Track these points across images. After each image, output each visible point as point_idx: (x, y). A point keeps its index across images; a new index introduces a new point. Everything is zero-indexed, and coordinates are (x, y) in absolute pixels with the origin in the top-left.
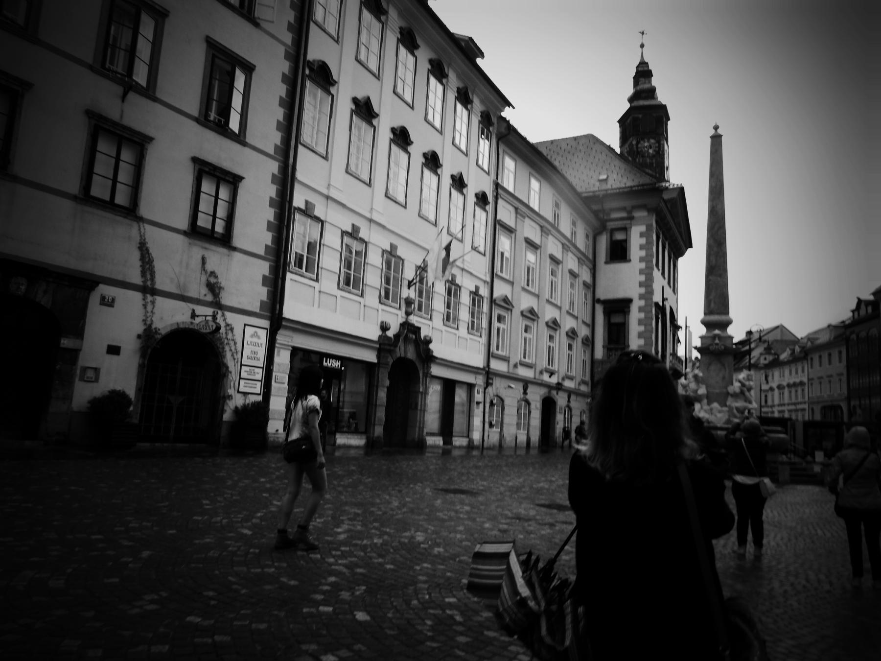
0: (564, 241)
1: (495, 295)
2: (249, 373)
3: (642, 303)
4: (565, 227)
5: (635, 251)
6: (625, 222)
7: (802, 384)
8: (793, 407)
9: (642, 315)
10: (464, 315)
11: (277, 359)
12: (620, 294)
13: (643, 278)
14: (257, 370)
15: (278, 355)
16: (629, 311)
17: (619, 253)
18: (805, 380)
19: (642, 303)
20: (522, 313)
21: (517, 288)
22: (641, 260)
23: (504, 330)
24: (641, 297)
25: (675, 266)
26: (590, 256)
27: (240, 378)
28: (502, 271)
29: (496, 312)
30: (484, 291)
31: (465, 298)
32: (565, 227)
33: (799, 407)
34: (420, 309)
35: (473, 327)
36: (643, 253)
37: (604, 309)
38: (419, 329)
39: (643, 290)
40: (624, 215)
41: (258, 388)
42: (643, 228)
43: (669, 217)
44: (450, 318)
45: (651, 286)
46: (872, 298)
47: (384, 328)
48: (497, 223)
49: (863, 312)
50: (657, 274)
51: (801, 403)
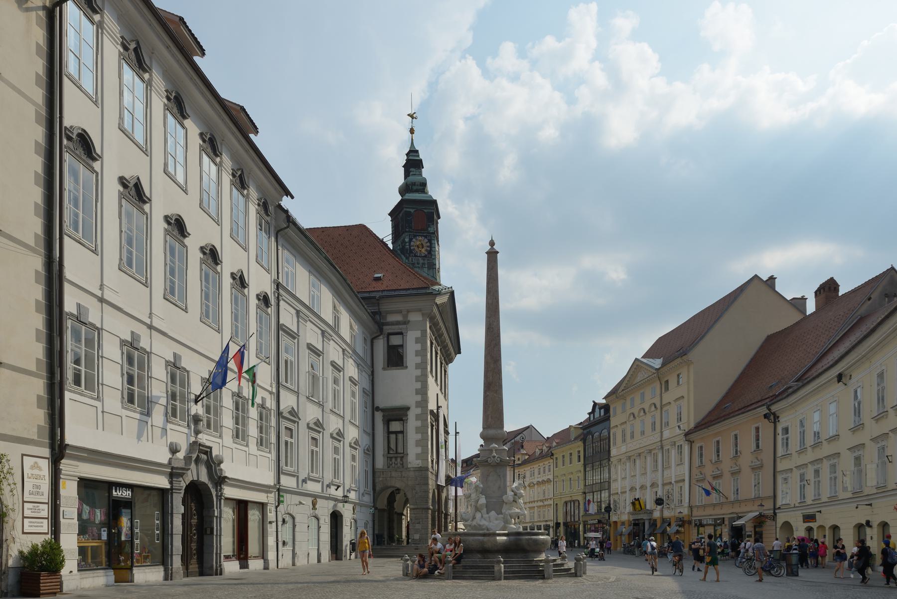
0: (345, 347)
1: (281, 408)
2: (33, 510)
3: (419, 411)
4: (345, 331)
5: (411, 358)
7: (549, 481)
10: (253, 430)
11: (63, 492)
12: (397, 402)
14: (41, 506)
15: (64, 488)
17: (396, 358)
18: (551, 477)
19: (419, 411)
20: (308, 424)
21: (302, 399)
22: (418, 366)
23: (291, 443)
24: (418, 404)
25: (445, 371)
26: (369, 362)
27: (24, 517)
28: (286, 382)
29: (284, 424)
30: (270, 403)
31: (253, 413)
32: (345, 331)
33: (546, 503)
34: (209, 426)
35: (261, 443)
37: (383, 416)
38: (211, 448)
39: (419, 398)
41: (45, 526)
43: (441, 324)
44: (239, 435)
45: (426, 394)
46: (604, 401)
47: (174, 450)
48: (279, 327)
49: (597, 415)
50: (431, 380)
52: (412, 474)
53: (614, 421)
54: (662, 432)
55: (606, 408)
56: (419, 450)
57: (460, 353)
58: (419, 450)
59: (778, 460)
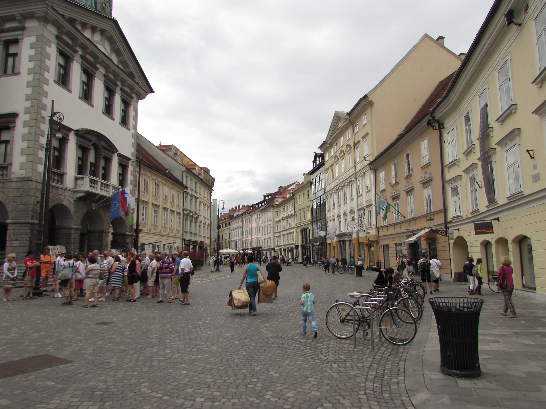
3: (27, 117)
6: (17, 33)
7: (292, 215)
8: (288, 232)
9: (26, 130)
13: (29, 91)
16: (14, 127)
19: (27, 117)
22: (30, 72)
25: (126, 104)
33: (291, 231)
36: (31, 65)
39: (28, 104)
40: (15, 25)
42: (33, 39)
46: (319, 152)
51: (292, 228)
52: (14, 185)
53: (327, 165)
54: (355, 166)
55: (322, 156)
56: (24, 159)
57: (152, 92)
58: (24, 159)
59: (446, 169)
